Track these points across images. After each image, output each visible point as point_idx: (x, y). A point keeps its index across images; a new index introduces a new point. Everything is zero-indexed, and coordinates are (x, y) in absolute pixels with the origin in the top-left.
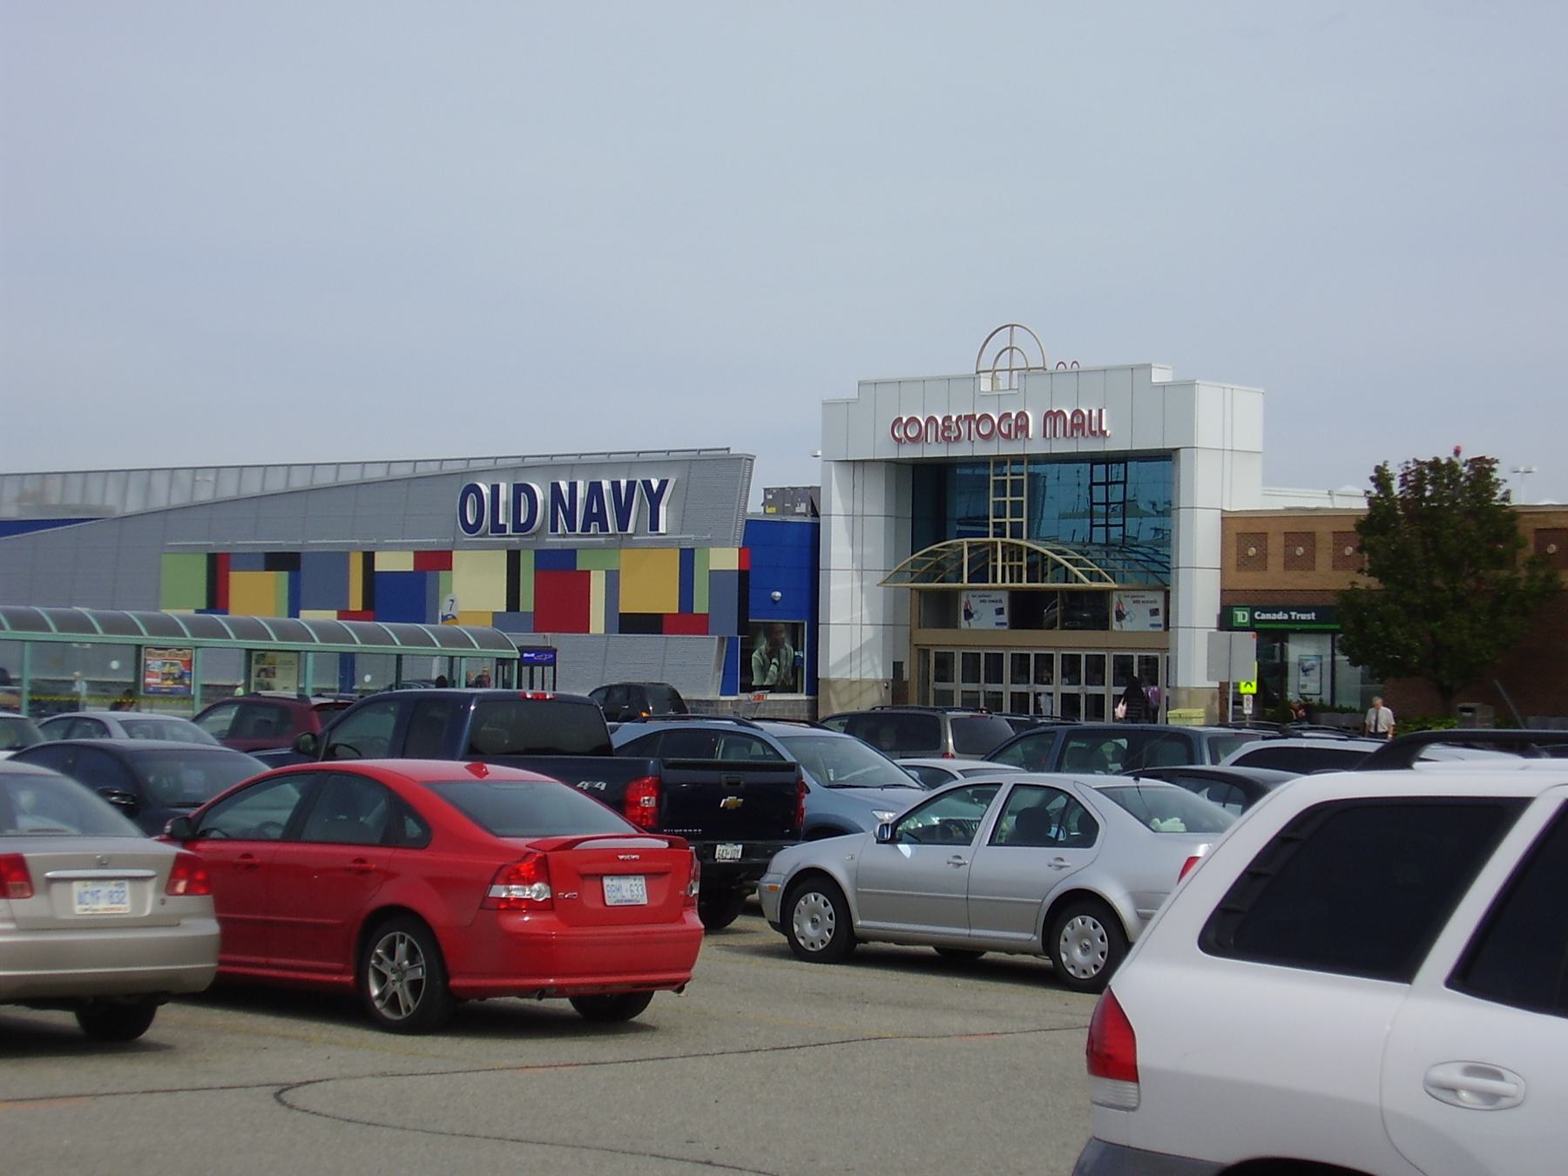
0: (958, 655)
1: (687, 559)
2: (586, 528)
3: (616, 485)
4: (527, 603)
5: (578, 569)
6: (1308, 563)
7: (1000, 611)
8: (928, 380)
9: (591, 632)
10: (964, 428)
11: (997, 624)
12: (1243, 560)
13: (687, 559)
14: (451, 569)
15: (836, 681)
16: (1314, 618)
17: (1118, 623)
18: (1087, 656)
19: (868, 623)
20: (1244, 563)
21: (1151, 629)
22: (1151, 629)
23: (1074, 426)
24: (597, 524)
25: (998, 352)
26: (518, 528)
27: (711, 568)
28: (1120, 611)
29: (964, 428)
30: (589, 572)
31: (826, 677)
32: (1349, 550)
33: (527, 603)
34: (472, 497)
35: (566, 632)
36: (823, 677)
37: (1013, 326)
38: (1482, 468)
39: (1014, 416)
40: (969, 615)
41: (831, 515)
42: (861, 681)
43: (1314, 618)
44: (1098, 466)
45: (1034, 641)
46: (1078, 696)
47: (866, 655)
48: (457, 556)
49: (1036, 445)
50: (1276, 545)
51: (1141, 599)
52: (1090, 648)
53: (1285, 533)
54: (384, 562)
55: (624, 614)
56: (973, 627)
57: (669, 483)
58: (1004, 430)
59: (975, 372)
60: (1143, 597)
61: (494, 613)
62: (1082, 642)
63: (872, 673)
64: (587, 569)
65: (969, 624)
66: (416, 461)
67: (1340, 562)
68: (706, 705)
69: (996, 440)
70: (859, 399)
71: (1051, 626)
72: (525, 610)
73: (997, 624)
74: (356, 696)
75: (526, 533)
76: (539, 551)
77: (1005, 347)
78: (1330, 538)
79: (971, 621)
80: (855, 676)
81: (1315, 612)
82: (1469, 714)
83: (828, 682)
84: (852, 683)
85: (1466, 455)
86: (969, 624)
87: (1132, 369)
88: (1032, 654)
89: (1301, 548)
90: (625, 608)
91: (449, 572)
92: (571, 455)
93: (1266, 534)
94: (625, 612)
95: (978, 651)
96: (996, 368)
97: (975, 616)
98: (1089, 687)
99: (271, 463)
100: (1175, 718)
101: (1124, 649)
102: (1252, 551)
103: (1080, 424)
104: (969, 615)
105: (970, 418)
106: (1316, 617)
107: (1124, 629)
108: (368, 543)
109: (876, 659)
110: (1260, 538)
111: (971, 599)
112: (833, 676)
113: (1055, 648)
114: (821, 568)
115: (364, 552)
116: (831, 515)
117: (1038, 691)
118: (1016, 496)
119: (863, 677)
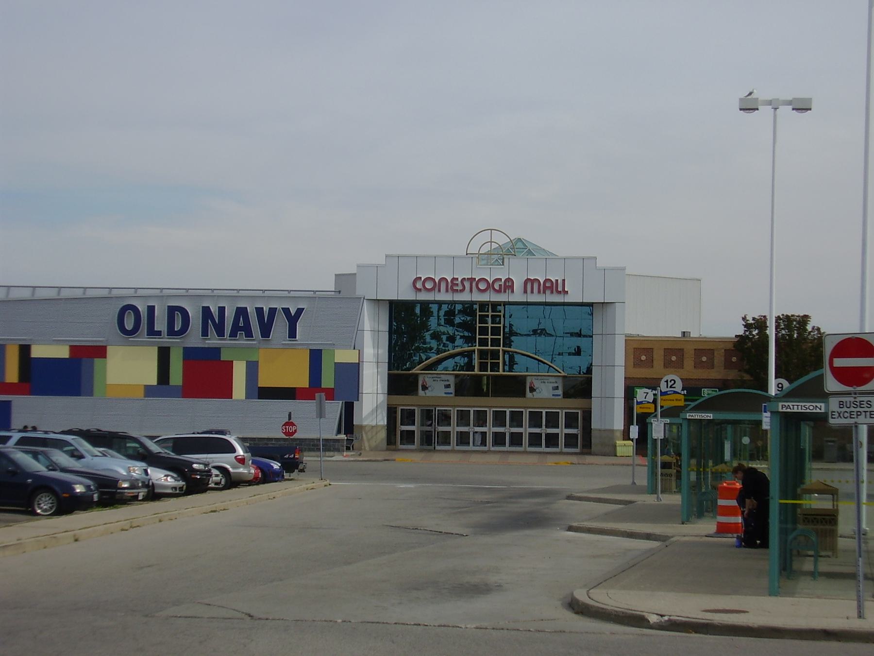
0: (562, 413)
1: (316, 357)
2: (233, 334)
3: (259, 311)
4: (176, 377)
5: (222, 359)
6: (710, 365)
7: (448, 386)
8: (419, 257)
9: (233, 398)
10: (467, 285)
11: (553, 395)
12: (637, 362)
13: (316, 357)
14: (105, 357)
15: (366, 426)
16: (685, 393)
17: (530, 394)
18: (546, 412)
19: (381, 392)
20: (638, 363)
21: (445, 395)
22: (445, 395)
23: (545, 288)
24: (239, 332)
25: (484, 242)
26: (171, 332)
27: (335, 361)
28: (532, 387)
29: (467, 285)
30: (232, 361)
31: (361, 424)
32: (734, 359)
33: (176, 377)
34: (177, 314)
35: (202, 398)
36: (356, 424)
37: (491, 230)
38: (805, 319)
39: (503, 280)
40: (425, 388)
41: (364, 330)
42: (377, 426)
43: (685, 393)
44: (508, 306)
45: (472, 404)
46: (504, 434)
47: (379, 411)
48: (110, 350)
49: (517, 296)
50: (659, 357)
51: (546, 381)
52: (548, 408)
53: (665, 349)
54: (38, 352)
55: (260, 387)
56: (427, 395)
57: (284, 307)
58: (497, 287)
59: (465, 254)
60: (548, 380)
61: (145, 385)
62: (508, 405)
63: (382, 421)
64: (230, 359)
65: (425, 393)
66: (34, 287)
67: (728, 365)
68: (333, 442)
69: (489, 291)
70: (385, 265)
71: (486, 395)
72: (333, 385)
73: (553, 395)
74: (249, 442)
75: (136, 335)
76: (162, 347)
77: (499, 243)
78: (693, 352)
79: (426, 391)
80: (374, 423)
81: (687, 391)
82: (832, 444)
83: (361, 427)
84: (373, 427)
85: (778, 310)
86: (425, 393)
87: (565, 259)
88: (472, 410)
89: (674, 357)
90: (261, 384)
91: (104, 359)
92: (199, 289)
93: (653, 349)
94: (261, 386)
95: (541, 410)
96: (480, 252)
97: (537, 390)
98: (547, 429)
99: (294, 289)
100: (622, 446)
101: (443, 406)
102: (643, 358)
103: (550, 286)
104: (425, 388)
105: (471, 280)
106: (687, 393)
107: (535, 397)
108: (24, 339)
109: (384, 412)
110: (649, 351)
111: (427, 379)
112: (365, 423)
113: (524, 408)
114: (387, 364)
115: (310, 350)
116: (364, 330)
117: (476, 430)
118: (482, 324)
119: (378, 424)
